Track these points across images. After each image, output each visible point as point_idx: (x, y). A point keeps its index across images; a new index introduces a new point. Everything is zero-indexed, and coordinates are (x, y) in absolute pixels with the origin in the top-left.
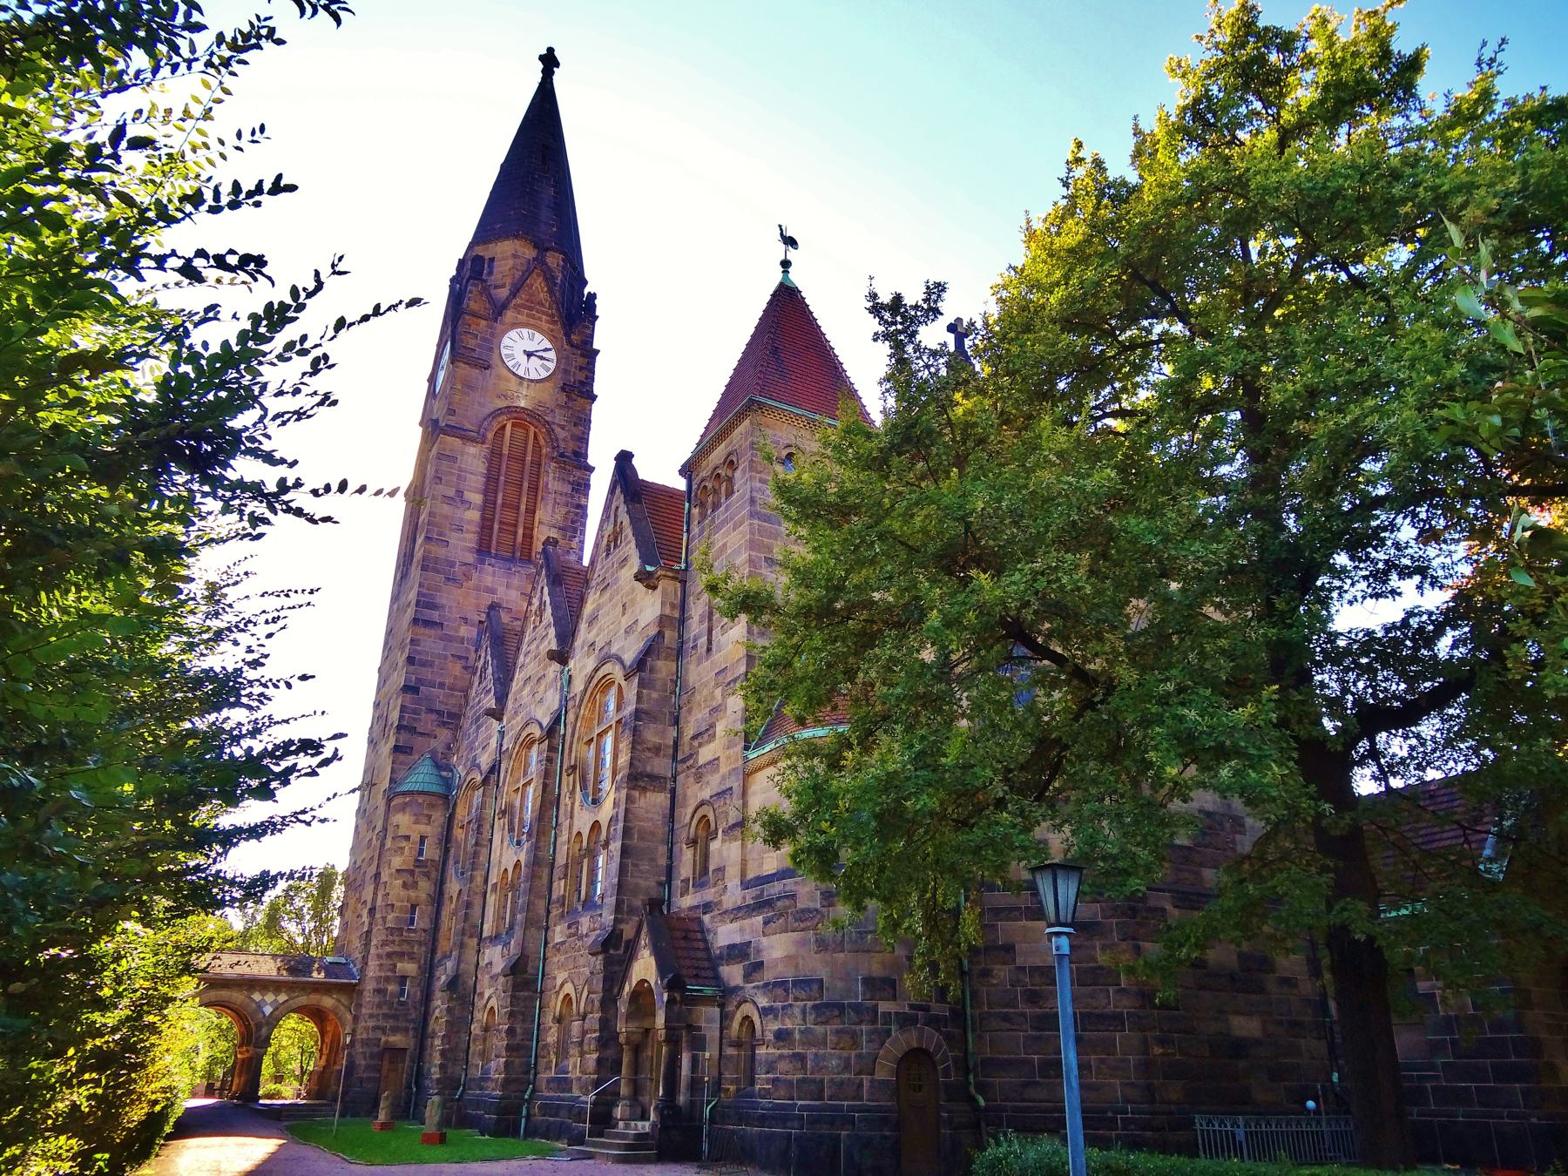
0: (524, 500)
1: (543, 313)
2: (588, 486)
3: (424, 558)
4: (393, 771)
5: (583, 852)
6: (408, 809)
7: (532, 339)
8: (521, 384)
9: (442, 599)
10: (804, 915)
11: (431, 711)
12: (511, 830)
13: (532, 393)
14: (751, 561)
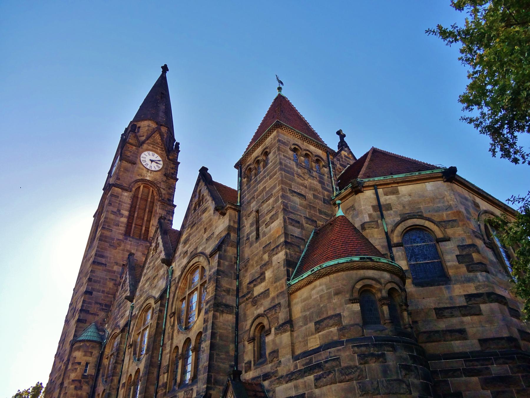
0: (146, 216)
1: (159, 147)
2: (173, 213)
3: (101, 236)
4: (75, 331)
5: (179, 357)
6: (81, 349)
7: (153, 155)
8: (148, 171)
9: (107, 254)
10: (346, 371)
11: (96, 303)
12: (135, 354)
13: (152, 176)
14: (282, 189)
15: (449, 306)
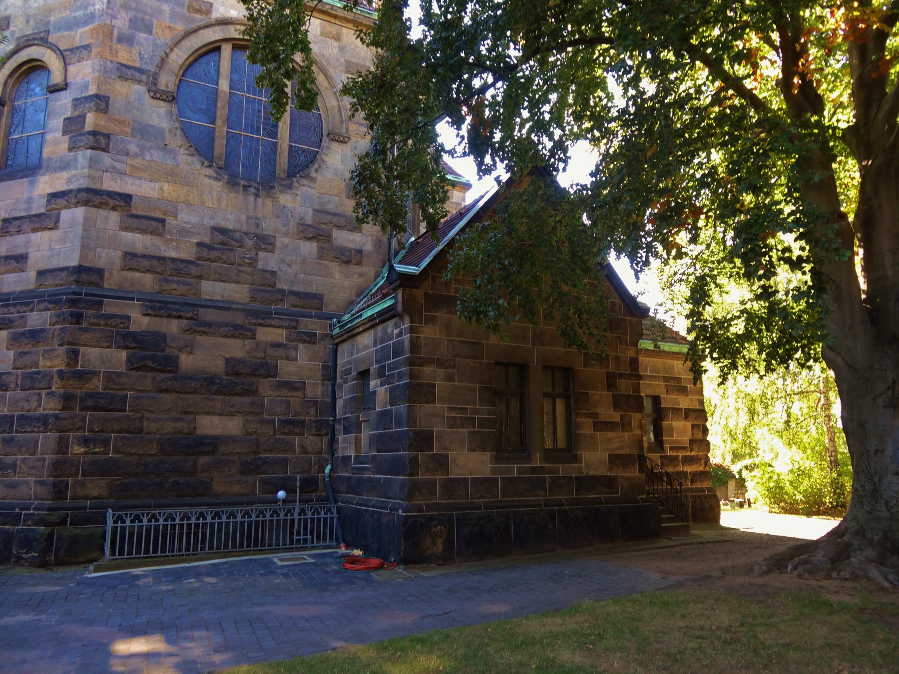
15: (23, 214)
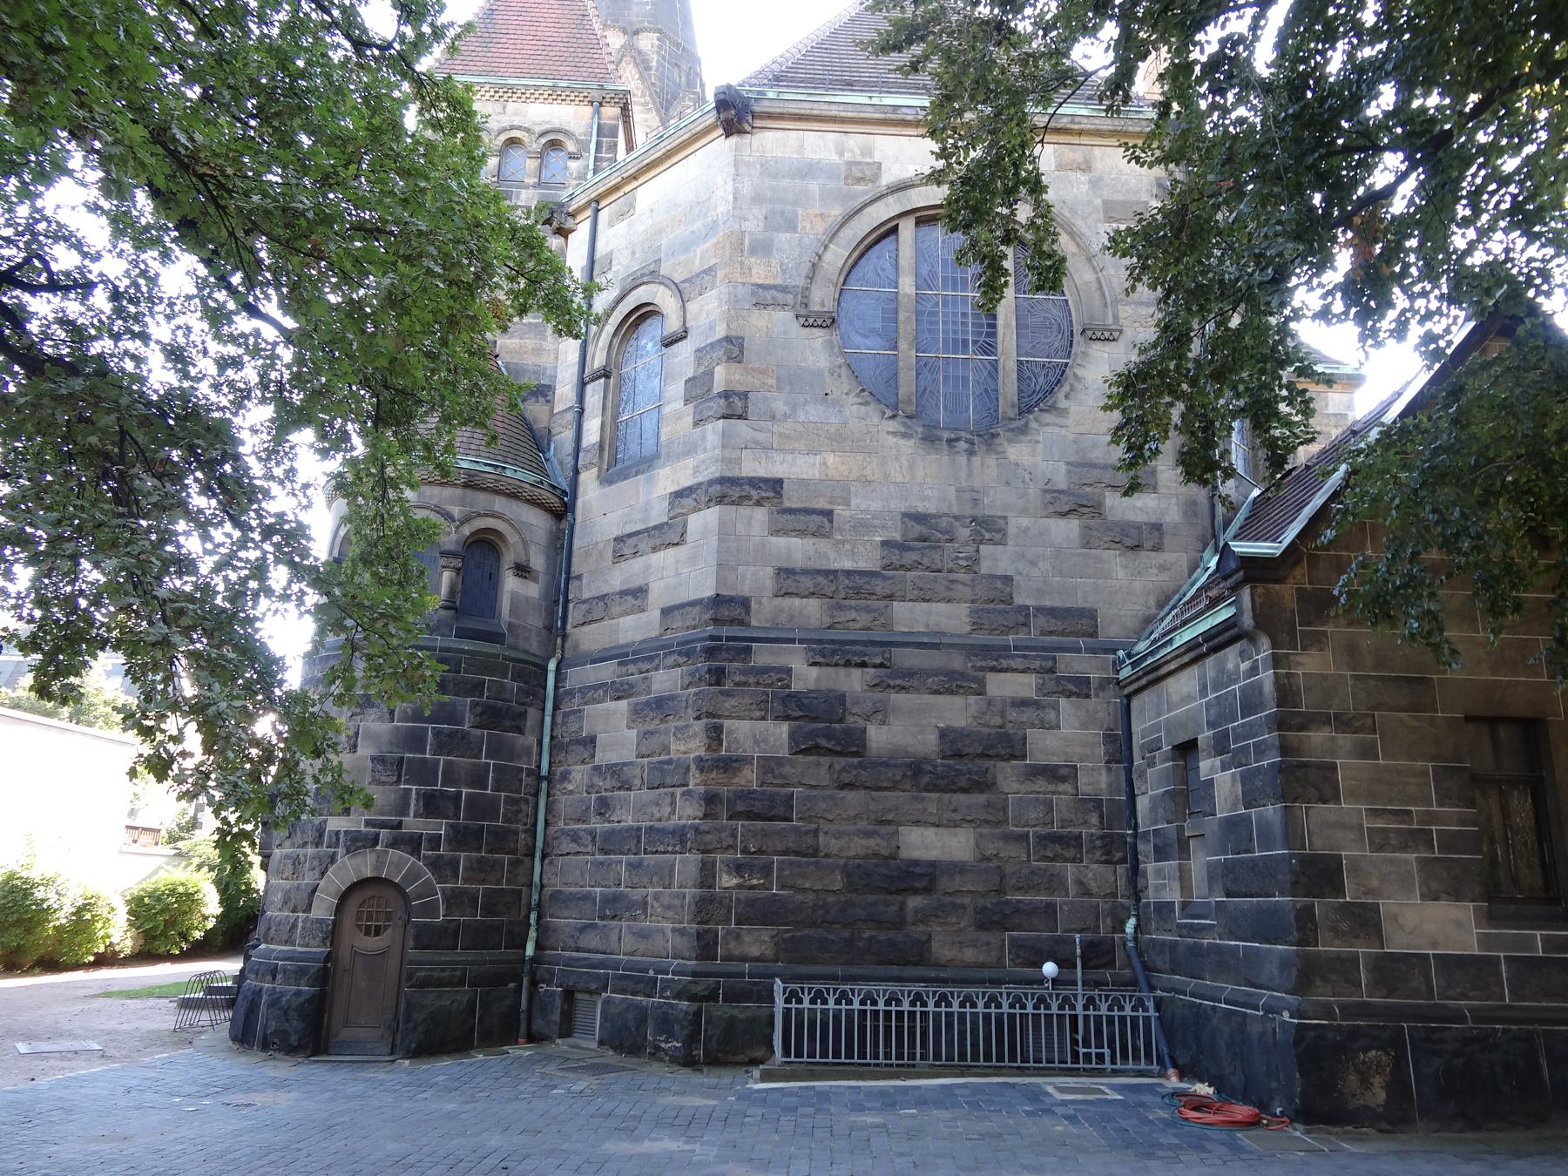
15: (639, 527)
